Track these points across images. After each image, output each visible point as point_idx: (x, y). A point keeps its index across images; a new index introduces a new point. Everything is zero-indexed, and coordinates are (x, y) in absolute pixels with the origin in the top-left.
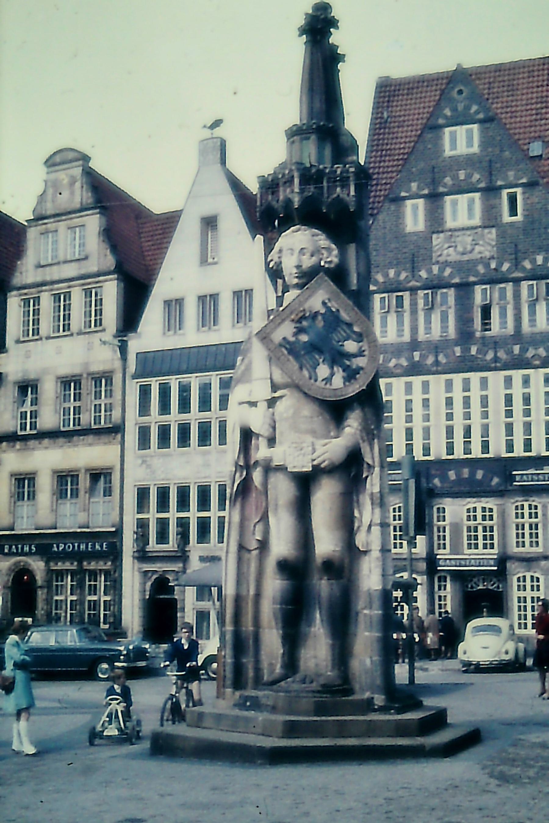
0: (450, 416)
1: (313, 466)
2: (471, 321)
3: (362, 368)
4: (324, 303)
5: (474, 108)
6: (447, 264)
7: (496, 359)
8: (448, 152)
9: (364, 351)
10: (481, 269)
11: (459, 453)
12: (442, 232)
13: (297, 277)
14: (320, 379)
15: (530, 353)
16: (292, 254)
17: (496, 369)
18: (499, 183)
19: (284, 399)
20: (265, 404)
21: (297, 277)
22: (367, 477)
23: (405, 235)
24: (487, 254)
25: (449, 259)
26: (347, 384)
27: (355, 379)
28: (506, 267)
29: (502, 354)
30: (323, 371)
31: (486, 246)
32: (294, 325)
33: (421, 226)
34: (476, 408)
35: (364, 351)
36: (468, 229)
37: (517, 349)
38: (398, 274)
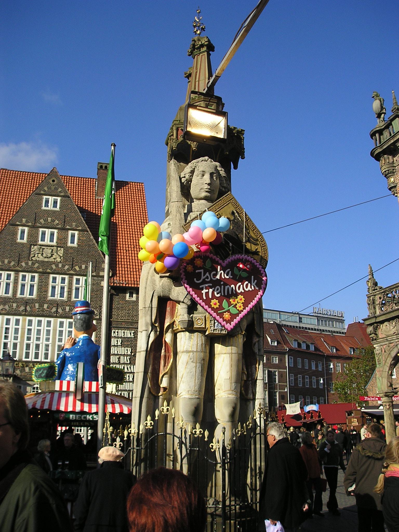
0: (29, 339)
2: (47, 291)
4: (233, 213)
5: (60, 190)
8: (44, 208)
9: (258, 252)
10: (54, 267)
11: (32, 358)
12: (36, 245)
13: (207, 192)
16: (203, 175)
17: (56, 317)
18: (68, 227)
21: (207, 192)
23: (16, 244)
24: (59, 260)
25: (38, 259)
28: (67, 267)
33: (25, 240)
34: (43, 336)
36: (49, 246)
37: (67, 309)
38: (9, 262)
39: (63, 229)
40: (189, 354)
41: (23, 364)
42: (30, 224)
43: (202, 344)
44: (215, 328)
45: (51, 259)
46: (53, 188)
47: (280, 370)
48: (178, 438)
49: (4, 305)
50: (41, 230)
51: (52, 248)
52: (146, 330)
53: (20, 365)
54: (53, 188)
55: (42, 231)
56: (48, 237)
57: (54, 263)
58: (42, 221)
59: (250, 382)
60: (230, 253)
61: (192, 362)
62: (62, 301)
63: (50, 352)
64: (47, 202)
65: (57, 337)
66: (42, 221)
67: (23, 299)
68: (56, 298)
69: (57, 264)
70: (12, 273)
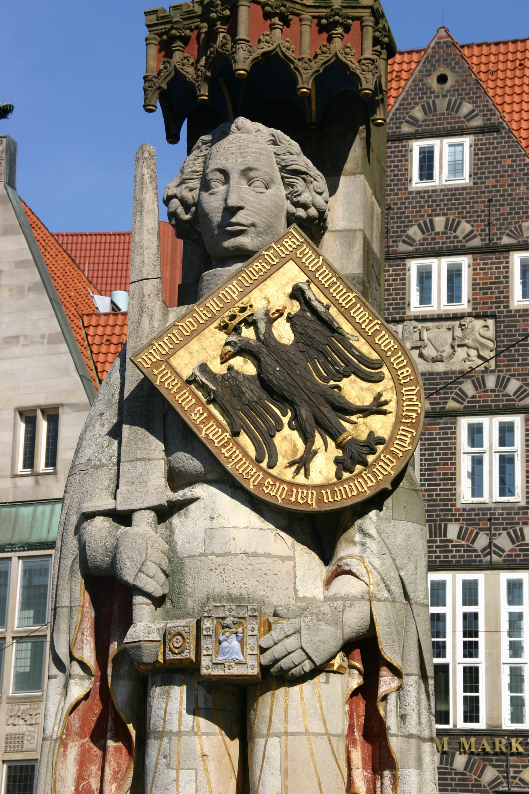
1: (261, 666)
2: (451, 478)
3: (381, 441)
4: (297, 294)
5: (466, 108)
8: (416, 183)
9: (386, 403)
10: (468, 388)
12: (402, 321)
14: (282, 461)
17: (492, 567)
18: (506, 240)
19: (192, 507)
20: (151, 515)
22: (385, 698)
26: (346, 475)
27: (365, 464)
28: (514, 385)
29: (503, 541)
32: (223, 337)
35: (386, 403)
39: (492, 251)
44: (220, 659)
46: (442, 105)
50: (414, 266)
51: (457, 323)
54: (442, 105)
55: (419, 268)
58: (414, 232)
60: (285, 420)
61: (168, 766)
62: (509, 508)
63: (482, 694)
65: (505, 641)
66: (414, 232)
68: (486, 498)
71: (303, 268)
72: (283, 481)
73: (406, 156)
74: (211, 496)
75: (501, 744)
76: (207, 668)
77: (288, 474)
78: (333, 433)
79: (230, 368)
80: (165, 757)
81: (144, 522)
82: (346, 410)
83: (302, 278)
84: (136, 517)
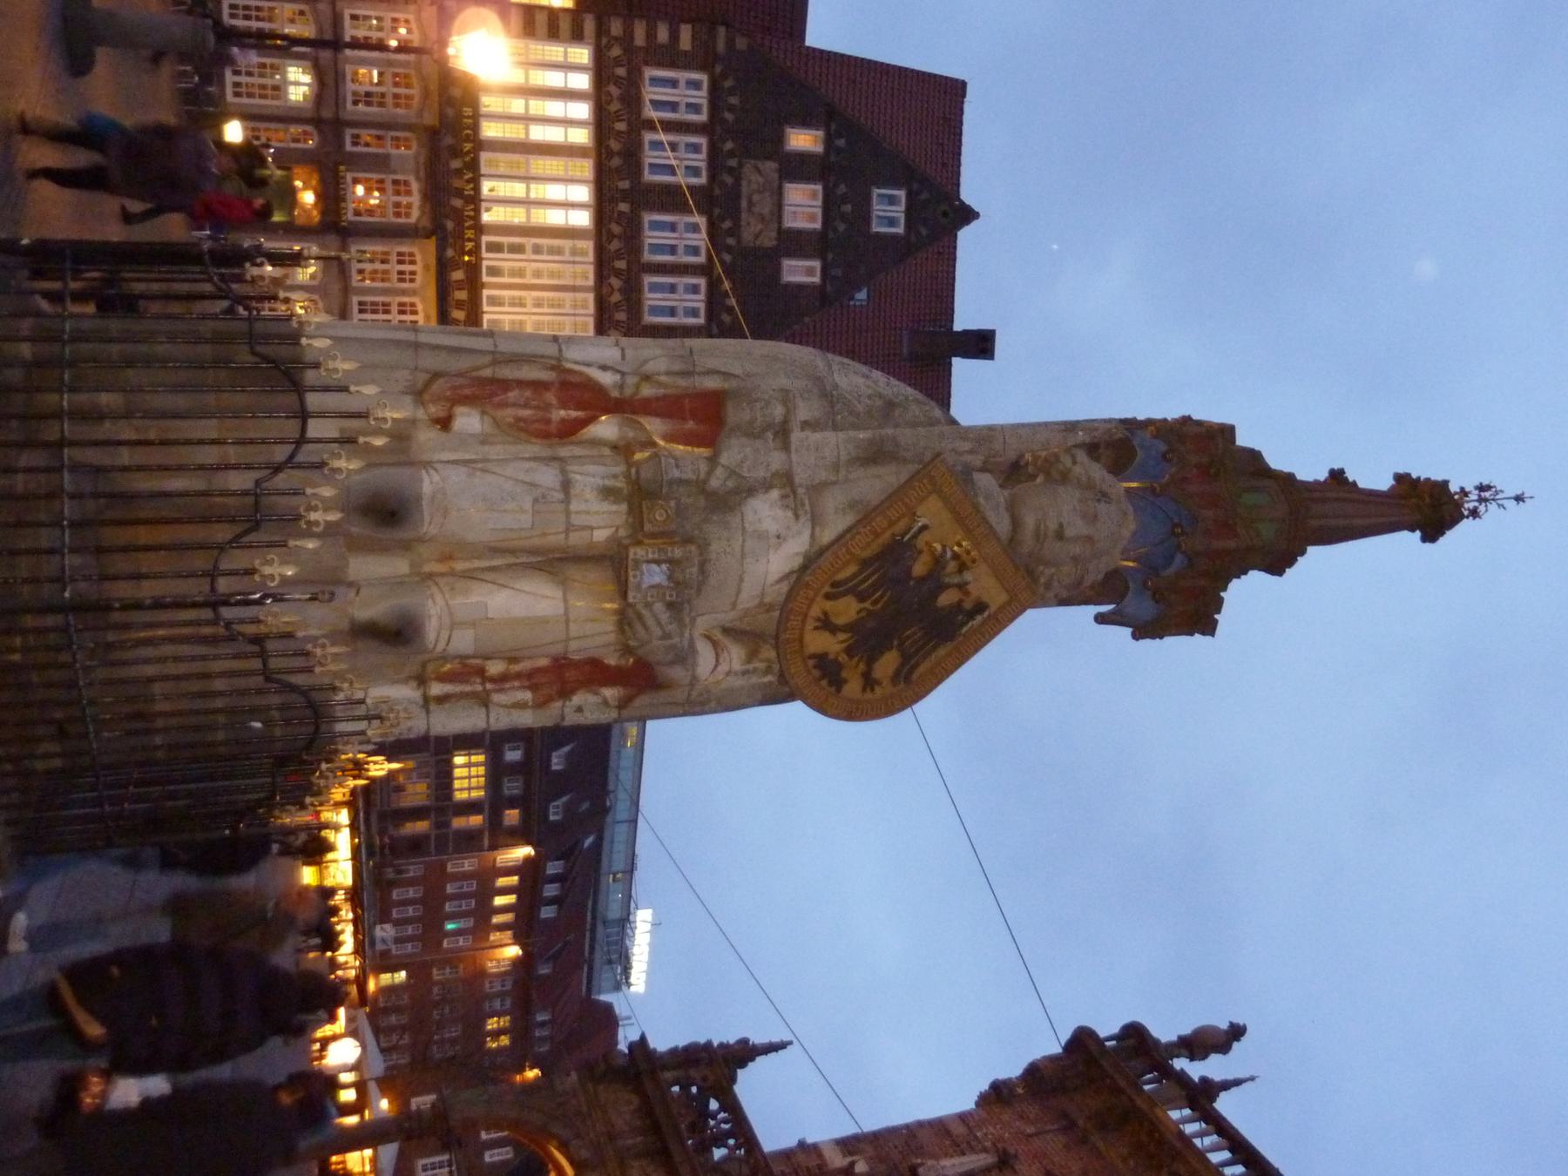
2: (663, 208)
3: (839, 690)
4: (980, 607)
6: (738, 180)
7: (611, 236)
8: (876, 191)
9: (872, 690)
10: (727, 224)
13: (1038, 528)
14: (828, 605)
15: (616, 282)
16: (1084, 516)
19: (790, 514)
25: (744, 183)
26: (811, 663)
29: (615, 245)
30: (847, 610)
31: (754, 232)
37: (621, 264)
38: (731, 109)
40: (558, 486)
41: (469, 152)
42: (833, 158)
43: (592, 528)
45: (744, 216)
47: (486, 834)
48: (292, 456)
49: (622, 99)
52: (623, 357)
53: (468, 146)
56: (803, 205)
57: (737, 225)
58: (842, 189)
59: (479, 688)
60: (867, 605)
61: (536, 501)
64: (892, 200)
66: (842, 189)
67: (640, 145)
68: (648, 233)
69: (735, 231)
70: (703, 117)
71: (1001, 608)
72: (809, 607)
73: (897, 186)
74: (799, 533)
75: (469, 234)
76: (636, 552)
77: (815, 611)
78: (849, 651)
79: (920, 552)
80: (544, 497)
81: (777, 460)
82: (870, 662)
83: (993, 609)
84: (783, 456)
